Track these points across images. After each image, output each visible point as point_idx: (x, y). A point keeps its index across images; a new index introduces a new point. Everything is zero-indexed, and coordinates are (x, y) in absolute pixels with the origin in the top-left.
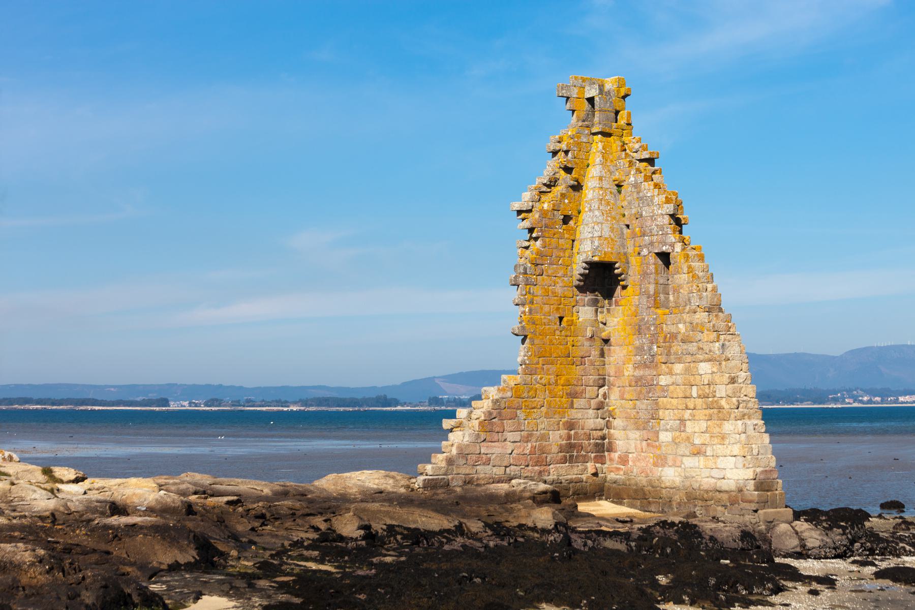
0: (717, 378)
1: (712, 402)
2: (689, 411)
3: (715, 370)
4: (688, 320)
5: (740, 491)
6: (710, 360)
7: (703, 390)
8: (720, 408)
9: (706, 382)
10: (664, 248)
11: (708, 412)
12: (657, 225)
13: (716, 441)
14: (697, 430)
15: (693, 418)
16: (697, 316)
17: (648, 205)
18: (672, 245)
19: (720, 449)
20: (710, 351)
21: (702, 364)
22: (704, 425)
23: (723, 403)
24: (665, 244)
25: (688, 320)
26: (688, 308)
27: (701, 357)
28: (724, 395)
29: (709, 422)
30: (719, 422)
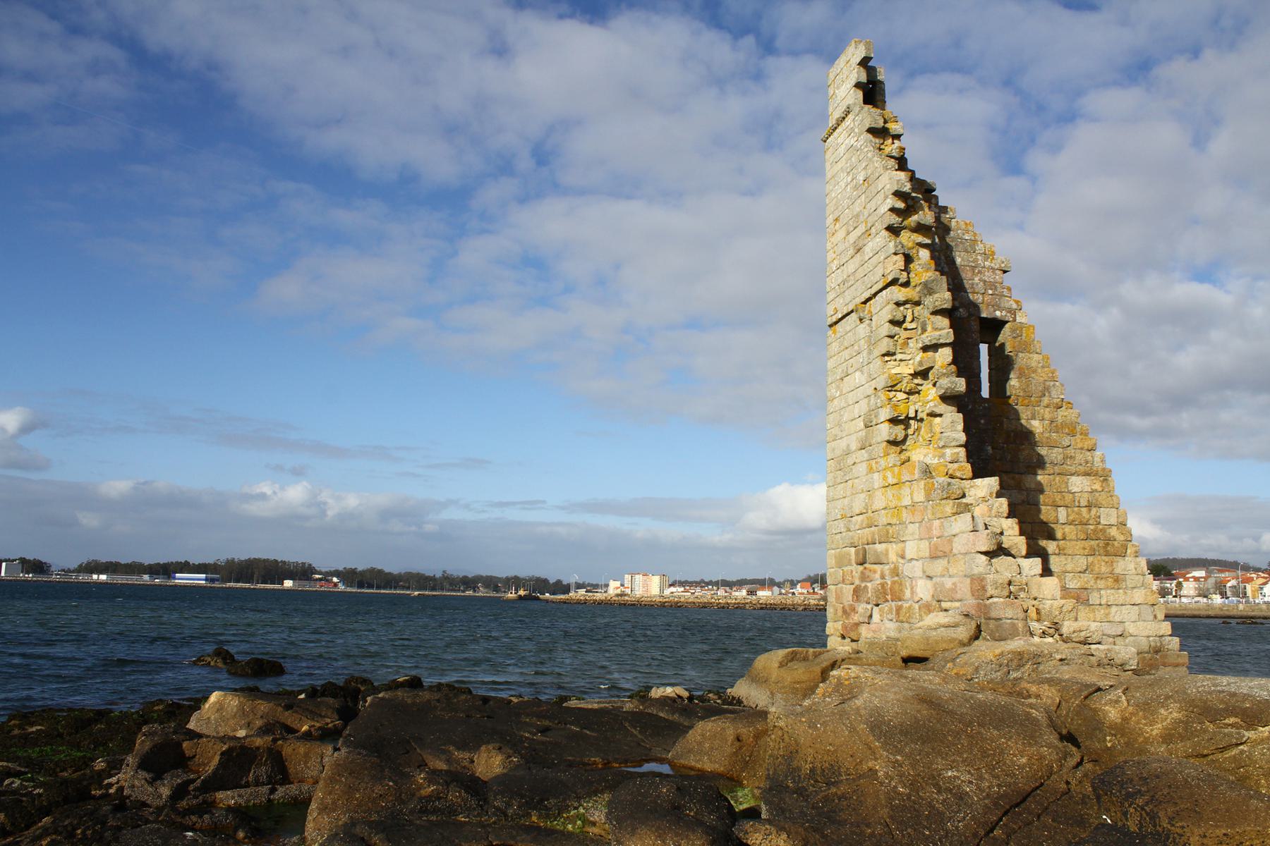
0: (1102, 498)
1: (1094, 531)
2: (1054, 543)
3: (1097, 486)
4: (1047, 416)
5: (1157, 651)
6: (1087, 474)
7: (1079, 514)
8: (1109, 540)
9: (1084, 503)
10: (998, 313)
11: (1088, 544)
12: (985, 282)
13: (1101, 584)
14: (1069, 568)
15: (1061, 552)
16: (1061, 412)
17: (966, 251)
18: (1013, 312)
19: (1108, 595)
20: (1087, 462)
21: (1073, 478)
22: (1082, 562)
23: (1113, 532)
24: (1001, 309)
25: (1047, 416)
26: (1046, 400)
27: (1073, 469)
28: (1113, 521)
29: (1091, 559)
30: (1106, 559)
